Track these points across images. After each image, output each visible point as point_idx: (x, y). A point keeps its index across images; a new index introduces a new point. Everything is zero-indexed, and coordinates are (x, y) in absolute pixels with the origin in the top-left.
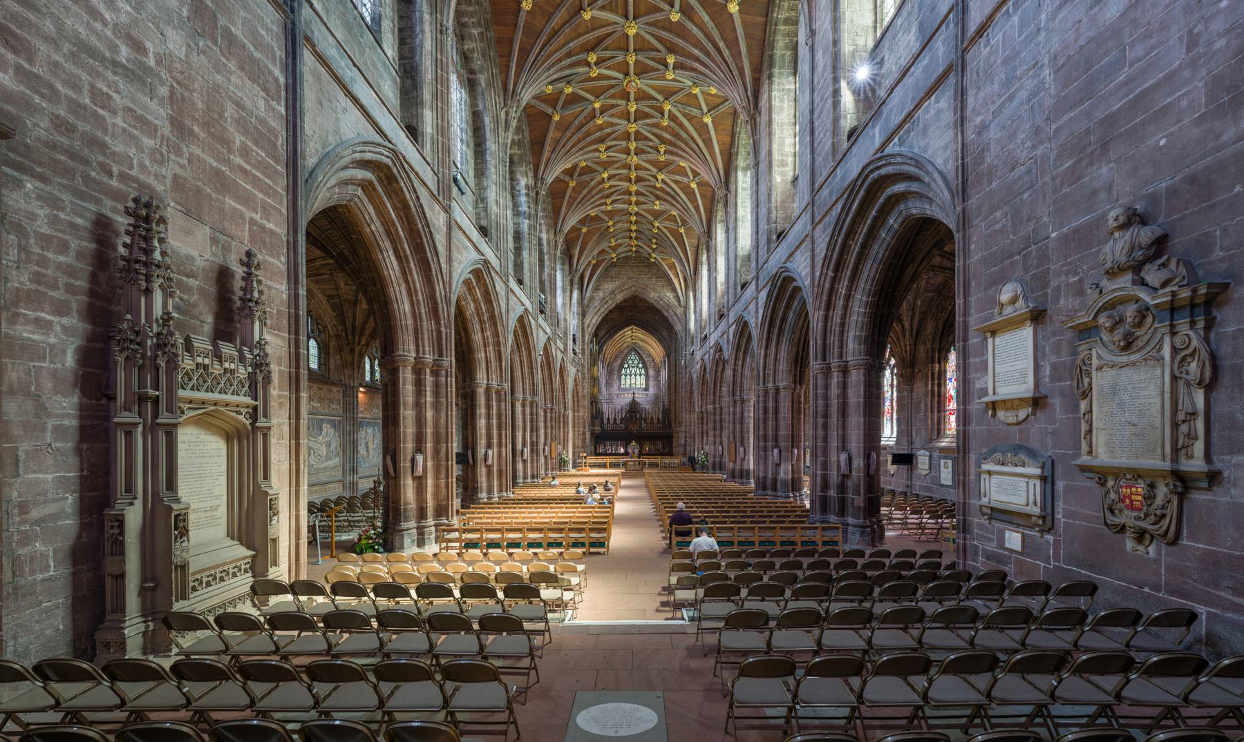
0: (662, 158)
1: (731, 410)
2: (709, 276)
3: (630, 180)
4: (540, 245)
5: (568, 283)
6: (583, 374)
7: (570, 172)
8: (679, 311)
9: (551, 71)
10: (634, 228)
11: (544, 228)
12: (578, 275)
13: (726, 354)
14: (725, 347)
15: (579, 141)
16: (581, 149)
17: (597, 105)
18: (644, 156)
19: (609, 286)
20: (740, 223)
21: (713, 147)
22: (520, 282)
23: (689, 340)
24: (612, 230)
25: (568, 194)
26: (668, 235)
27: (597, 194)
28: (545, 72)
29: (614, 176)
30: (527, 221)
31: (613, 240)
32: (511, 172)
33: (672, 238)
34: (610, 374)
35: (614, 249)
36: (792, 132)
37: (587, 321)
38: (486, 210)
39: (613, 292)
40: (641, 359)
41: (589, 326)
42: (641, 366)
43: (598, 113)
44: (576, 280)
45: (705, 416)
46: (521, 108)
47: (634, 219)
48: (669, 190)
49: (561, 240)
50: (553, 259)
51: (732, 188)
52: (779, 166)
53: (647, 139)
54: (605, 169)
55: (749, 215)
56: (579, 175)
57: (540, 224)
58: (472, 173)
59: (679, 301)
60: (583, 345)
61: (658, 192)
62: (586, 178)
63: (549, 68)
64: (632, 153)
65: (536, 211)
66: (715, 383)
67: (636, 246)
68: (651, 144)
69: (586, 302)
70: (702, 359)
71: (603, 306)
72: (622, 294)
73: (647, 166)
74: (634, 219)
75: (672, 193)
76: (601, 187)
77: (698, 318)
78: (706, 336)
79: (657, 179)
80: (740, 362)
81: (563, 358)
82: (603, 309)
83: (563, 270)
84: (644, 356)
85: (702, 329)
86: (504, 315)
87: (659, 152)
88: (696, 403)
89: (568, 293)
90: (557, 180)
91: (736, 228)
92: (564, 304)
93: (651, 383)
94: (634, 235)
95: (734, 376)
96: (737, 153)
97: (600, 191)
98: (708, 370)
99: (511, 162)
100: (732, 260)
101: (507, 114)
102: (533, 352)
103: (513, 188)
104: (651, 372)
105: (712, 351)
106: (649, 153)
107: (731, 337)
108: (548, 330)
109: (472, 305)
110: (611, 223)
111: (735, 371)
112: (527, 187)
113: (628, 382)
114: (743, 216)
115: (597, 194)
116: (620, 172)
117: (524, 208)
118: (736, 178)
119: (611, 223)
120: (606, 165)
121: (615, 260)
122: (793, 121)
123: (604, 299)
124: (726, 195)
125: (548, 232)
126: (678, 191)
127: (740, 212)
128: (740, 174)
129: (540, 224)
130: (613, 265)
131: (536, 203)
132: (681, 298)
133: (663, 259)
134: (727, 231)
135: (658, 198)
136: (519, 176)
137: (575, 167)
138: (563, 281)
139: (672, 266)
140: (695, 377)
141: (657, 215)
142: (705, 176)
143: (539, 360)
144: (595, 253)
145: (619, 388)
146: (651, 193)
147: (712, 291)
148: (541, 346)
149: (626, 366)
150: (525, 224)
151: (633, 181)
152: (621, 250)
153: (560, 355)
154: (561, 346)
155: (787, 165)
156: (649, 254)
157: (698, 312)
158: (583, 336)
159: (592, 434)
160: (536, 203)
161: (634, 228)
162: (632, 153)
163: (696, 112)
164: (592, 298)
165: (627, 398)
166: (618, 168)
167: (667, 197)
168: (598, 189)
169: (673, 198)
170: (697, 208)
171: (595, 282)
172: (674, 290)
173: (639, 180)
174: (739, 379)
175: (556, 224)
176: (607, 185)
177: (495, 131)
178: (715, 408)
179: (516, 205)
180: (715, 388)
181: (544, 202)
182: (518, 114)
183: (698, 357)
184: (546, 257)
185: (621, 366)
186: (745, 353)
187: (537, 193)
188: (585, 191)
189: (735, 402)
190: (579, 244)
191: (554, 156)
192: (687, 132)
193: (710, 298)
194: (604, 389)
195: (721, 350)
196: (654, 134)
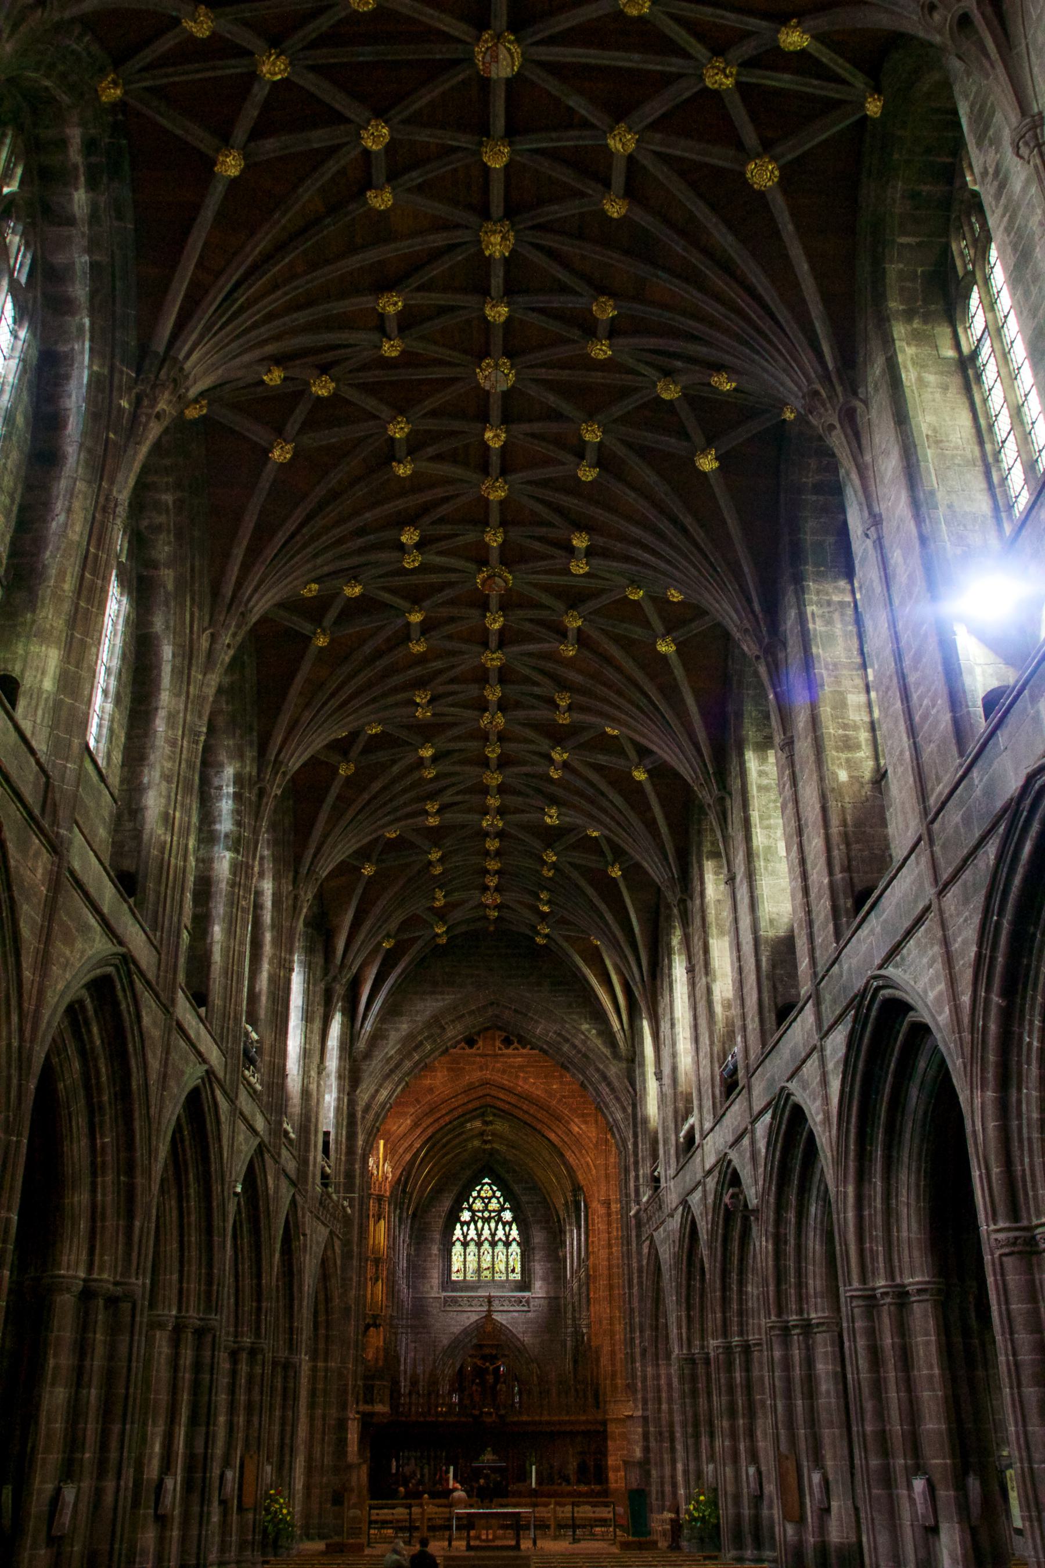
0: (564, 719)
1: (777, 1354)
2: (692, 984)
3: (485, 763)
4: (258, 906)
5: (319, 998)
6: (347, 1243)
7: (341, 747)
8: (614, 1070)
9: (319, 561)
10: (493, 865)
11: (268, 865)
12: (348, 976)
13: (752, 1193)
14: (746, 1174)
15: (370, 685)
16: (374, 700)
17: (416, 618)
18: (521, 714)
19: (427, 1007)
20: (760, 864)
21: (682, 701)
22: (200, 998)
23: (644, 1148)
24: (438, 870)
25: (334, 791)
26: (583, 883)
27: (404, 791)
28: (308, 561)
29: (448, 753)
30: (228, 855)
31: (439, 894)
32: (207, 749)
33: (590, 891)
34: (419, 1238)
35: (441, 915)
36: (859, 682)
37: (363, 1096)
38: (137, 834)
39: (436, 1022)
40: (509, 1195)
41: (367, 1108)
42: (507, 1216)
43: (415, 633)
44: (340, 989)
45: (701, 1370)
46: (246, 629)
47: (492, 845)
48: (579, 784)
49: (308, 895)
50: (284, 942)
51: (735, 785)
52: (838, 749)
53: (527, 680)
54: (427, 740)
55: (781, 846)
56: (366, 751)
57: (262, 858)
58: (117, 757)
59: (612, 1043)
60: (350, 1161)
61: (553, 789)
62: (382, 756)
63: (316, 556)
64: (493, 707)
65: (256, 831)
66: (725, 1273)
67: (498, 907)
68: (537, 690)
69: (362, 1045)
70: (684, 1203)
71: (409, 1055)
72: (459, 1027)
73: (530, 734)
74: (492, 845)
75: (590, 792)
76: (416, 775)
77: (668, 1090)
78: (690, 1137)
79: (552, 761)
80: (791, 1216)
81: (293, 1202)
82: (408, 1064)
83: (309, 967)
84: (516, 1188)
85: (681, 1115)
86: (153, 1090)
87: (557, 706)
88: (674, 1331)
89: (317, 1025)
90: (313, 763)
91: (751, 876)
92: (306, 1054)
93: (538, 1268)
94: (492, 882)
95: (778, 1254)
96: (739, 715)
97: (413, 786)
98: (703, 1236)
99: (212, 729)
100: (748, 948)
101: (213, 638)
102: (217, 1188)
103: (205, 782)
104: (538, 1237)
105: (711, 1183)
106: (533, 707)
107: (762, 1145)
108: (260, 1124)
109: (76, 1065)
110: (435, 856)
111: (779, 1240)
112: (238, 780)
113: (472, 1265)
114: (768, 848)
115: (404, 791)
116: (460, 745)
117: (225, 825)
118: (742, 764)
119: (435, 856)
120: (427, 732)
121: (443, 940)
122: (858, 660)
123: (410, 1036)
124: (721, 800)
125: (277, 878)
126: (604, 787)
127: (760, 838)
128: (752, 761)
129: (262, 858)
130: (438, 952)
131: (257, 816)
132: (620, 1036)
133: (567, 938)
134: (731, 880)
135: (554, 801)
136: (223, 757)
137: (354, 735)
138: (307, 993)
139: (596, 960)
140: (666, 1253)
141: (551, 836)
142: (667, 753)
143: (231, 1208)
144: (393, 926)
145: (447, 1283)
146: (539, 791)
147: (703, 1022)
148: (239, 1168)
149: (466, 1216)
150: (224, 862)
151: (493, 764)
152: (457, 915)
153: (286, 1193)
154: (291, 1166)
155: (858, 747)
156: (534, 928)
157: (668, 1075)
158: (351, 1136)
159: (367, 1422)
160: (257, 816)
161: (493, 865)
162: (493, 707)
163: (638, 633)
164: (377, 1037)
165: (470, 1317)
166: (459, 738)
167: (576, 800)
168: (408, 781)
169: (592, 802)
170: (651, 825)
171: (391, 993)
172: (599, 1016)
173: (504, 763)
174: (791, 1264)
175: (298, 859)
176: (430, 774)
177: (183, 674)
178: (728, 1349)
179: (208, 816)
180: (725, 1288)
181: (275, 812)
182: (239, 638)
183: (672, 1197)
184: (268, 937)
185: (453, 1218)
186: (803, 1190)
187: (261, 793)
188: (377, 786)
189: (786, 1330)
190: (354, 903)
191: (307, 715)
192: (619, 669)
193: (696, 1040)
194: (403, 1284)
195: (736, 1180)
196: (542, 672)
